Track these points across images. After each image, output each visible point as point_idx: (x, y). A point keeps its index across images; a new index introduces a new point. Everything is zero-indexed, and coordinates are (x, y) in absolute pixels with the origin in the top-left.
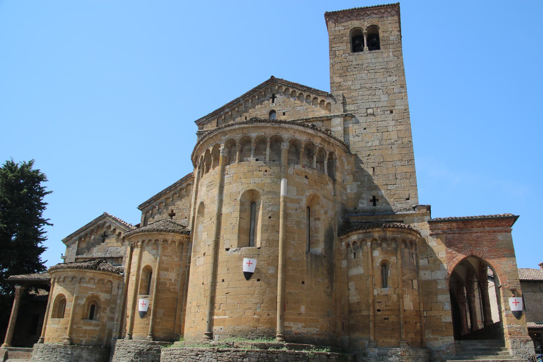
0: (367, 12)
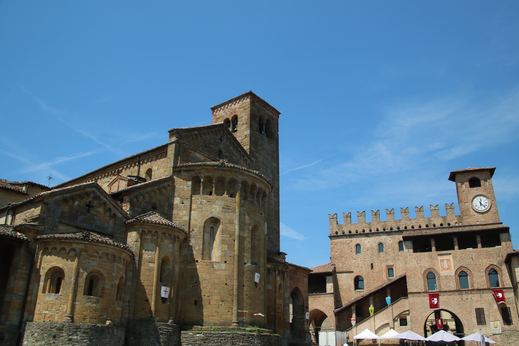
0: (268, 107)
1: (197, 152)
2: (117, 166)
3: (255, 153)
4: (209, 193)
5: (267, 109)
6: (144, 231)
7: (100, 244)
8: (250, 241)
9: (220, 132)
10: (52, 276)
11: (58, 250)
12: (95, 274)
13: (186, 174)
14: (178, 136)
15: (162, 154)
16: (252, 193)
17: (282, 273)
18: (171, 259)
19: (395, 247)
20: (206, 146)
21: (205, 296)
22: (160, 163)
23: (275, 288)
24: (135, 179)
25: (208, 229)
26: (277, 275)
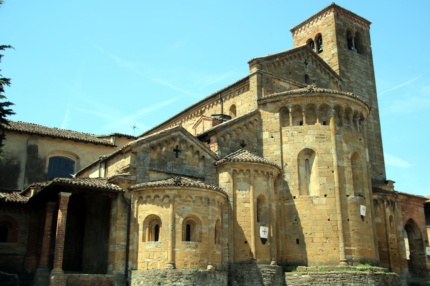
0: (355, 19)
1: (281, 81)
2: (199, 107)
3: (346, 73)
4: (299, 124)
5: (355, 21)
6: (236, 171)
7: (192, 188)
8: (351, 171)
9: (303, 54)
10: (149, 225)
11: (152, 198)
12: (190, 219)
13: (272, 106)
14: (258, 65)
15: (244, 87)
16: (348, 118)
17: (392, 204)
18: (267, 197)
20: (290, 73)
21: (307, 233)
22: (243, 97)
23: (385, 220)
24: (220, 118)
25: (303, 162)
26: (385, 207)
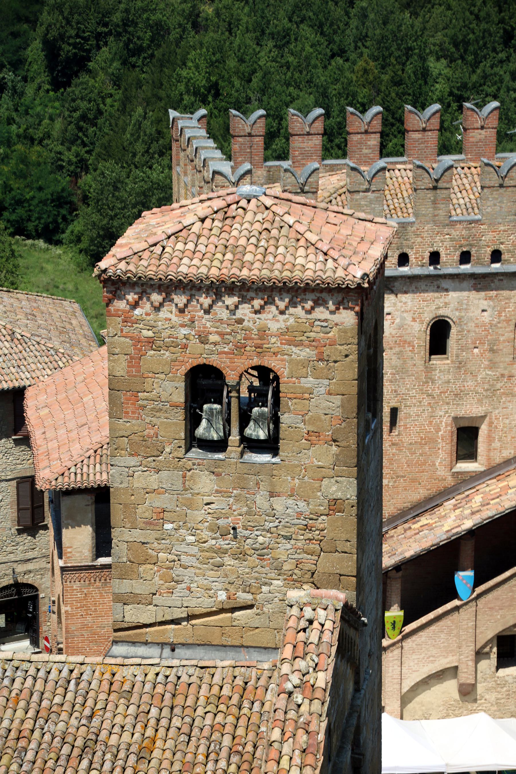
19: (502, 339)
